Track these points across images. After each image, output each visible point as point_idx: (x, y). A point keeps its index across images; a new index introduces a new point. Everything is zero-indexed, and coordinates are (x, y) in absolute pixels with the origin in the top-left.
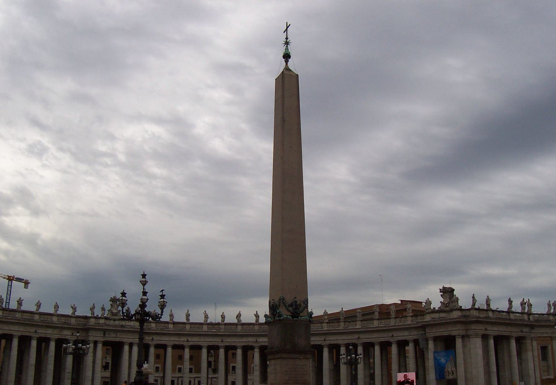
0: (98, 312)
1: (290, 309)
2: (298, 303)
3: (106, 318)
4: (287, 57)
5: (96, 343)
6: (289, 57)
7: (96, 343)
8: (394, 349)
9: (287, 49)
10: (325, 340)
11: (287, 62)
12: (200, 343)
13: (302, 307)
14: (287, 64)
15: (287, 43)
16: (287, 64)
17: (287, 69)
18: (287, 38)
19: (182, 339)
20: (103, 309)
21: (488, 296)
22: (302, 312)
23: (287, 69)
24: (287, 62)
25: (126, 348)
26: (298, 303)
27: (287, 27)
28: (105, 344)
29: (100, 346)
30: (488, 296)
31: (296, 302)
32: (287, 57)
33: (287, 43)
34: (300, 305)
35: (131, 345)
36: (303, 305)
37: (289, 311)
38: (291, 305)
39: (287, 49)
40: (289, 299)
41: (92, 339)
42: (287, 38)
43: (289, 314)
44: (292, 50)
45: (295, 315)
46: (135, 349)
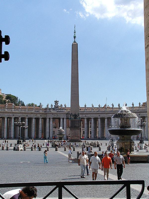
0: (50, 107)
3: (53, 109)
4: (75, 37)
5: (50, 119)
7: (50, 119)
10: (139, 115)
12: (91, 117)
15: (75, 32)
17: (75, 42)
18: (75, 31)
19: (83, 116)
20: (52, 105)
23: (75, 42)
28: (53, 118)
29: (51, 120)
33: (75, 32)
34: (77, 115)
35: (63, 119)
36: (78, 115)
38: (74, 115)
40: (73, 114)
41: (48, 117)
42: (75, 31)
45: (75, 118)
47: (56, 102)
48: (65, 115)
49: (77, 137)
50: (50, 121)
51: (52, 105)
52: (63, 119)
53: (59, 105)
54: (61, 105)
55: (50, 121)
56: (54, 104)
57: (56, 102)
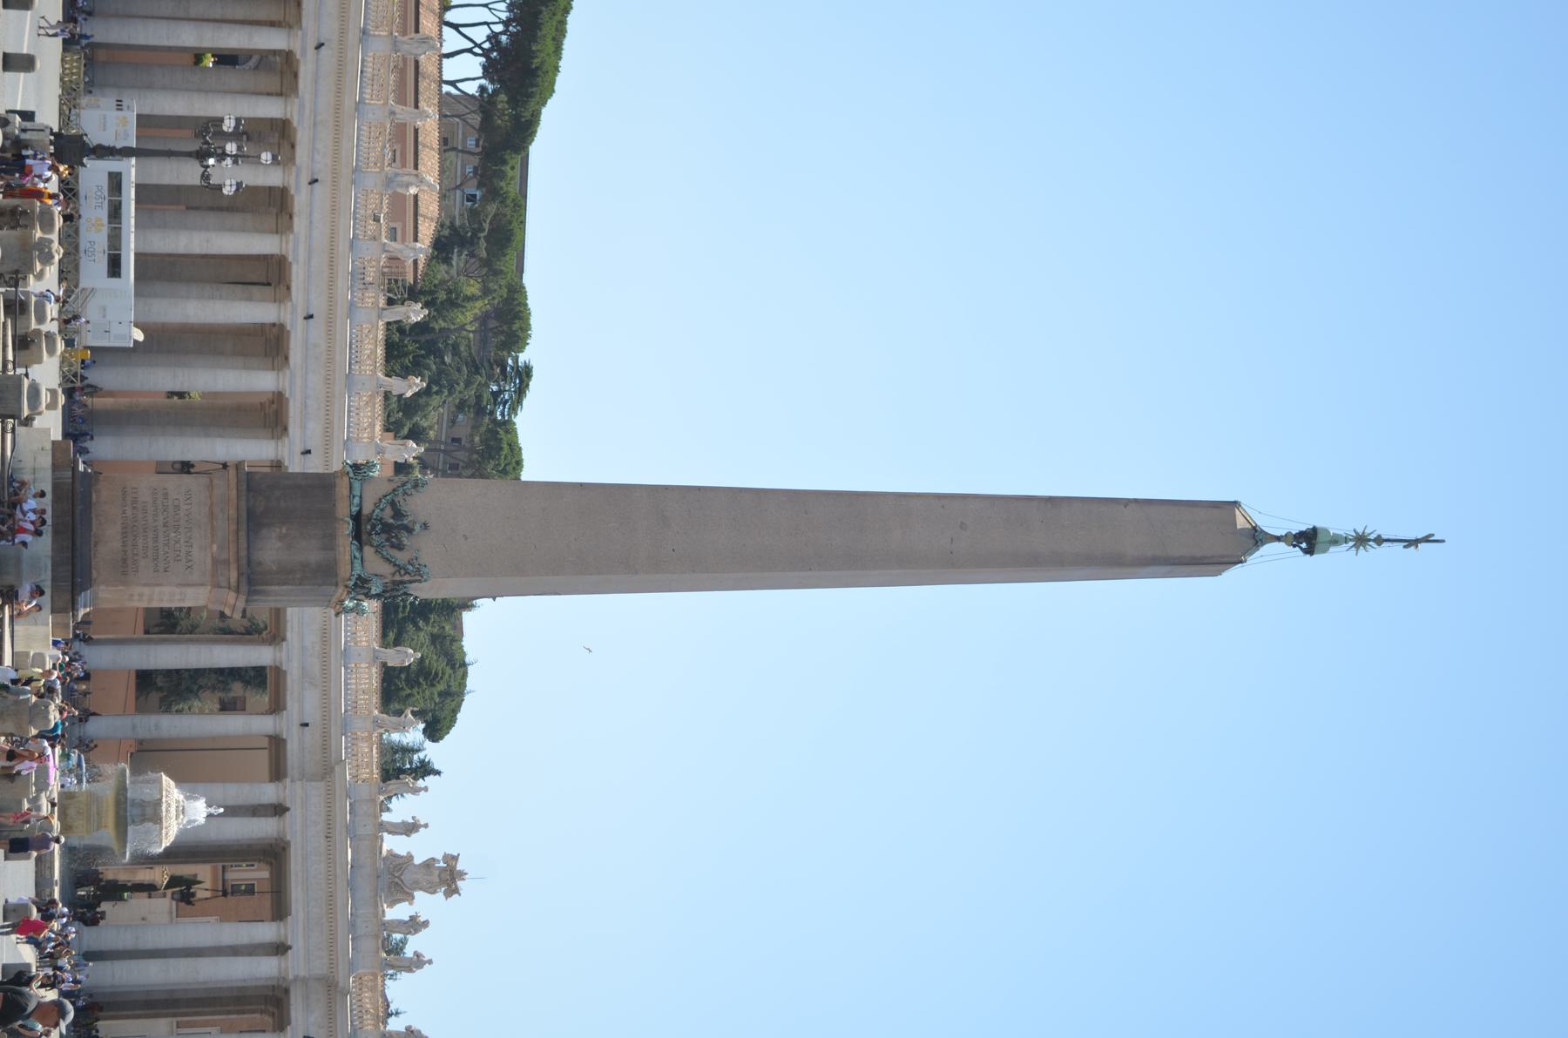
1: (389, 512)
2: (405, 539)
4: (1309, 541)
6: (1310, 551)
7: (279, 810)
9: (1336, 541)
13: (395, 553)
14: (1278, 539)
15: (1361, 540)
17: (1257, 537)
18: (1379, 541)
21: (438, 773)
22: (378, 549)
23: (1257, 537)
25: (266, 932)
26: (405, 539)
27: (1427, 539)
30: (438, 773)
31: (410, 530)
32: (1309, 541)
33: (1361, 540)
34: (400, 547)
35: (280, 949)
36: (401, 557)
37: (376, 505)
38: (398, 514)
39: (1336, 541)
42: (1379, 541)
46: (265, 968)
47: (446, 877)
48: (319, 967)
49: (117, 545)
50: (256, 811)
51: (410, 828)
52: (280, 949)
53: (424, 904)
54: (414, 925)
55: (256, 811)
56: (419, 848)
57: (446, 877)
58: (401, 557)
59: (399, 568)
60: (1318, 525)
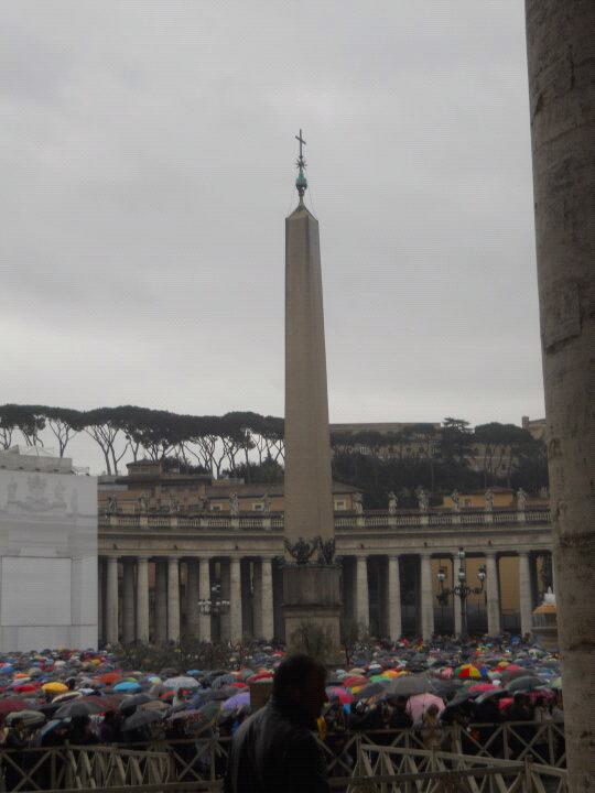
4: (301, 186)
8: (144, 574)
9: (301, 175)
11: (301, 194)
14: (301, 199)
15: (301, 165)
16: (301, 199)
17: (301, 208)
18: (301, 157)
23: (301, 208)
24: (301, 194)
32: (301, 186)
33: (301, 165)
36: (311, 546)
37: (294, 556)
39: (301, 175)
42: (301, 157)
43: (295, 560)
44: (307, 174)
58: (311, 546)
59: (315, 548)
60: (294, 183)
